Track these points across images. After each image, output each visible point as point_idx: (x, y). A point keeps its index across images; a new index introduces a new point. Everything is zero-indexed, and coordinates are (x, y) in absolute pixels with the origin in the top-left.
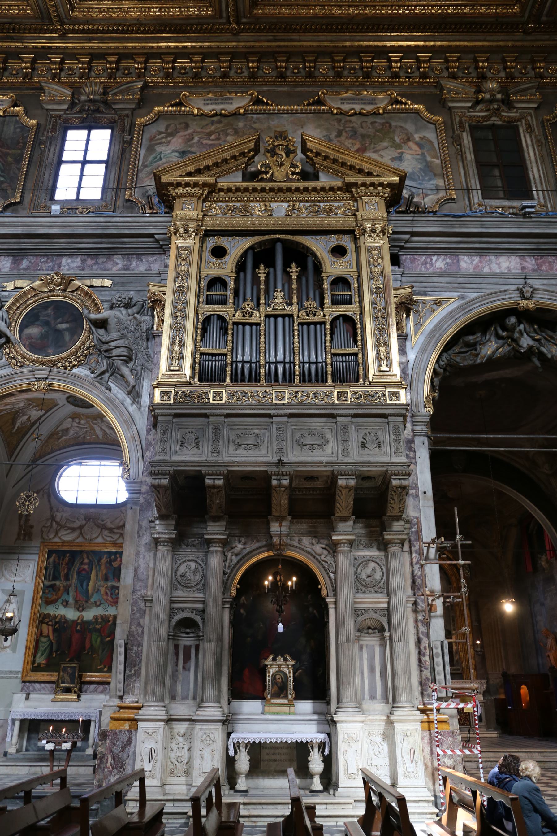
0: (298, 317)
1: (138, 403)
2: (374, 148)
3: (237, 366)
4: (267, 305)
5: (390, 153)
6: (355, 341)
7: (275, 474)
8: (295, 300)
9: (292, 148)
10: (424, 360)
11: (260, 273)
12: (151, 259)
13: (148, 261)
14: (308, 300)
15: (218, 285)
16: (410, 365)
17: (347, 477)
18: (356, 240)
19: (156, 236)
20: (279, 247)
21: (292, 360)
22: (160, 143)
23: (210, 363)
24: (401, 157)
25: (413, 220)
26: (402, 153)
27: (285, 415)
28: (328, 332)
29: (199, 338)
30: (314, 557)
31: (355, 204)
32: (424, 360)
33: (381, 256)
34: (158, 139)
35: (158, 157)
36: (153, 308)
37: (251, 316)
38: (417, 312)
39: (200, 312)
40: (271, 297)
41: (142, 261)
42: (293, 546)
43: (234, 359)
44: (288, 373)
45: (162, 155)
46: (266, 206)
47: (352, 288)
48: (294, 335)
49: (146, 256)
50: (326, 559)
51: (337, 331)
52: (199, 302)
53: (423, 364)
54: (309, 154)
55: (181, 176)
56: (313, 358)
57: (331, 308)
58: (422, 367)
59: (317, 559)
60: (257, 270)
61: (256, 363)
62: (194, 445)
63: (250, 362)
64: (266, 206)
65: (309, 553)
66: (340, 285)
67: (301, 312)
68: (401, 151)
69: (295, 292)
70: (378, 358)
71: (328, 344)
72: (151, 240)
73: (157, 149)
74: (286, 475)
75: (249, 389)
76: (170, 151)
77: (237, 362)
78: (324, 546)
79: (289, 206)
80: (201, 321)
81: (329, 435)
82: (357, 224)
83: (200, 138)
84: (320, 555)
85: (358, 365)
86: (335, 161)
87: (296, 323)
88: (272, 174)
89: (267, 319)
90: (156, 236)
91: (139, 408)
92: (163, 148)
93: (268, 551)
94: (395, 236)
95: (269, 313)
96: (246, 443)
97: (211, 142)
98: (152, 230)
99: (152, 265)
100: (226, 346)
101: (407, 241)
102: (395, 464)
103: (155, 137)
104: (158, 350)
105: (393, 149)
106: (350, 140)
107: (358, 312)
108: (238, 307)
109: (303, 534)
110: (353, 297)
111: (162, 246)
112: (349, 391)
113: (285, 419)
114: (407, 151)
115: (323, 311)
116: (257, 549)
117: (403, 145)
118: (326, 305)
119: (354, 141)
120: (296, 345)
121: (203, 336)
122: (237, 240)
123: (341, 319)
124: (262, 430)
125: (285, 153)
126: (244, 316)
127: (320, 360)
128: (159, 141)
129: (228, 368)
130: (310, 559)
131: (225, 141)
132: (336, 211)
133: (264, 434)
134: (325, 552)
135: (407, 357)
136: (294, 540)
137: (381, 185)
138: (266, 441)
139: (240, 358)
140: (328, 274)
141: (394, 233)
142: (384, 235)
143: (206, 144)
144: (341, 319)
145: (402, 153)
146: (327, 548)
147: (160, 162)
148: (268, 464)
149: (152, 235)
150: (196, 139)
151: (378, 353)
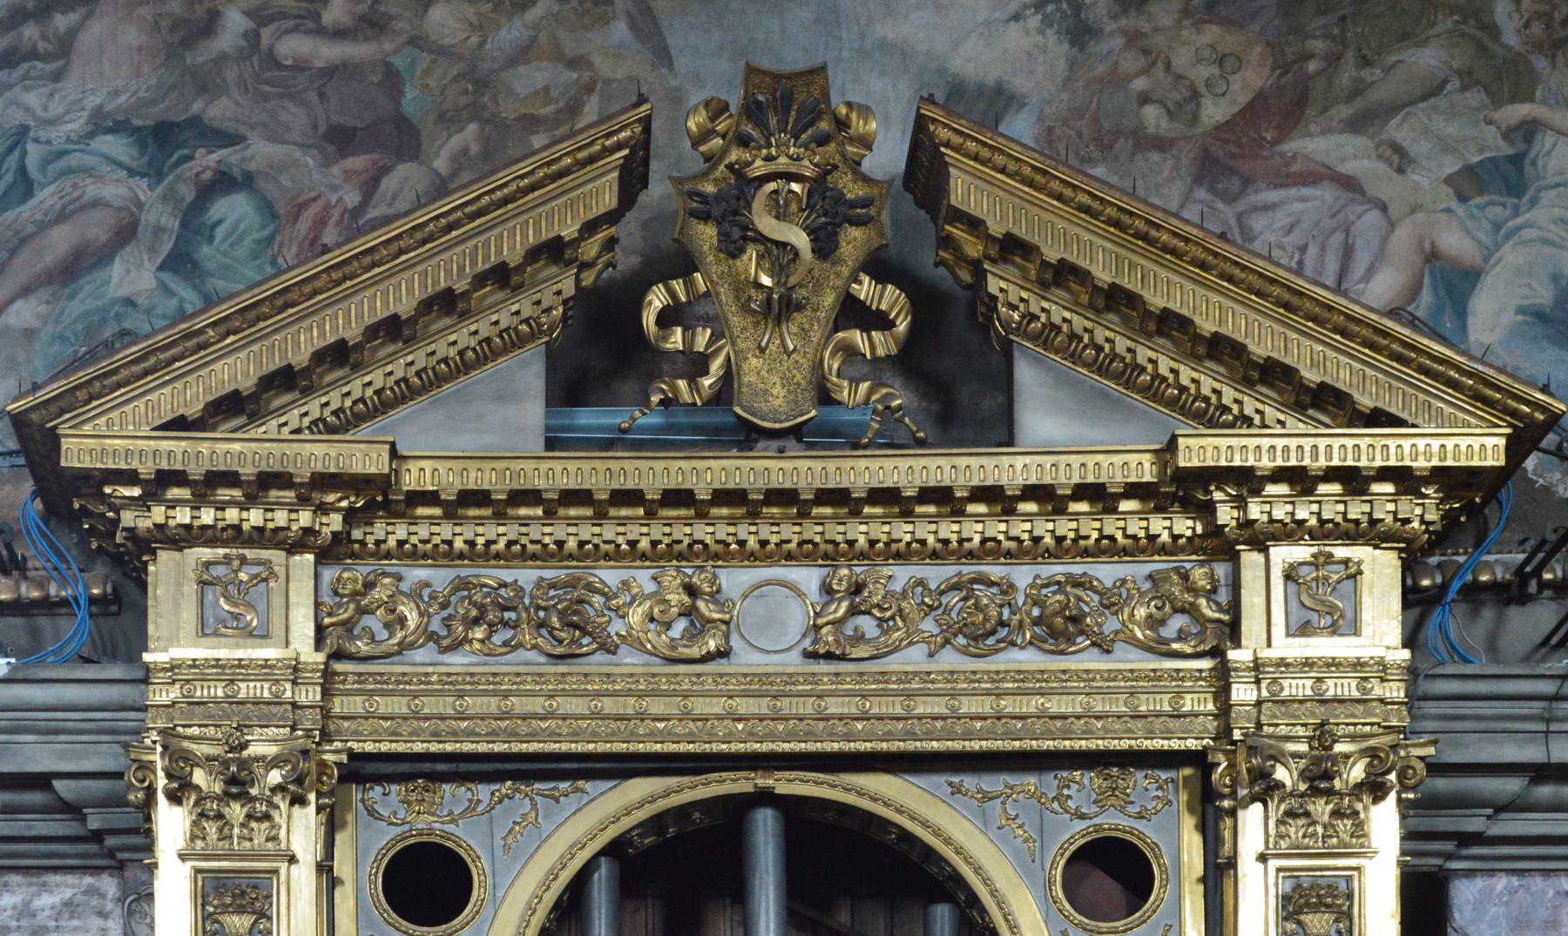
2: (1356, 92)
5: (1452, 129)
19: (57, 784)
24: (1517, 160)
26: (1529, 130)
31: (1221, 570)
45: (34, 154)
46: (691, 591)
68: (1518, 112)
76: (77, 125)
79: (827, 589)
83: (259, 16)
88: (728, 376)
90: (57, 784)
92: (33, 99)
97: (328, 52)
98: (38, 757)
105: (1476, 97)
106: (1212, 33)
117: (1540, 63)
119: (1230, 41)
132: (1111, 625)
141: (1436, 768)
143: (300, 66)
145: (1529, 130)
147: (26, 212)
150: (235, 22)
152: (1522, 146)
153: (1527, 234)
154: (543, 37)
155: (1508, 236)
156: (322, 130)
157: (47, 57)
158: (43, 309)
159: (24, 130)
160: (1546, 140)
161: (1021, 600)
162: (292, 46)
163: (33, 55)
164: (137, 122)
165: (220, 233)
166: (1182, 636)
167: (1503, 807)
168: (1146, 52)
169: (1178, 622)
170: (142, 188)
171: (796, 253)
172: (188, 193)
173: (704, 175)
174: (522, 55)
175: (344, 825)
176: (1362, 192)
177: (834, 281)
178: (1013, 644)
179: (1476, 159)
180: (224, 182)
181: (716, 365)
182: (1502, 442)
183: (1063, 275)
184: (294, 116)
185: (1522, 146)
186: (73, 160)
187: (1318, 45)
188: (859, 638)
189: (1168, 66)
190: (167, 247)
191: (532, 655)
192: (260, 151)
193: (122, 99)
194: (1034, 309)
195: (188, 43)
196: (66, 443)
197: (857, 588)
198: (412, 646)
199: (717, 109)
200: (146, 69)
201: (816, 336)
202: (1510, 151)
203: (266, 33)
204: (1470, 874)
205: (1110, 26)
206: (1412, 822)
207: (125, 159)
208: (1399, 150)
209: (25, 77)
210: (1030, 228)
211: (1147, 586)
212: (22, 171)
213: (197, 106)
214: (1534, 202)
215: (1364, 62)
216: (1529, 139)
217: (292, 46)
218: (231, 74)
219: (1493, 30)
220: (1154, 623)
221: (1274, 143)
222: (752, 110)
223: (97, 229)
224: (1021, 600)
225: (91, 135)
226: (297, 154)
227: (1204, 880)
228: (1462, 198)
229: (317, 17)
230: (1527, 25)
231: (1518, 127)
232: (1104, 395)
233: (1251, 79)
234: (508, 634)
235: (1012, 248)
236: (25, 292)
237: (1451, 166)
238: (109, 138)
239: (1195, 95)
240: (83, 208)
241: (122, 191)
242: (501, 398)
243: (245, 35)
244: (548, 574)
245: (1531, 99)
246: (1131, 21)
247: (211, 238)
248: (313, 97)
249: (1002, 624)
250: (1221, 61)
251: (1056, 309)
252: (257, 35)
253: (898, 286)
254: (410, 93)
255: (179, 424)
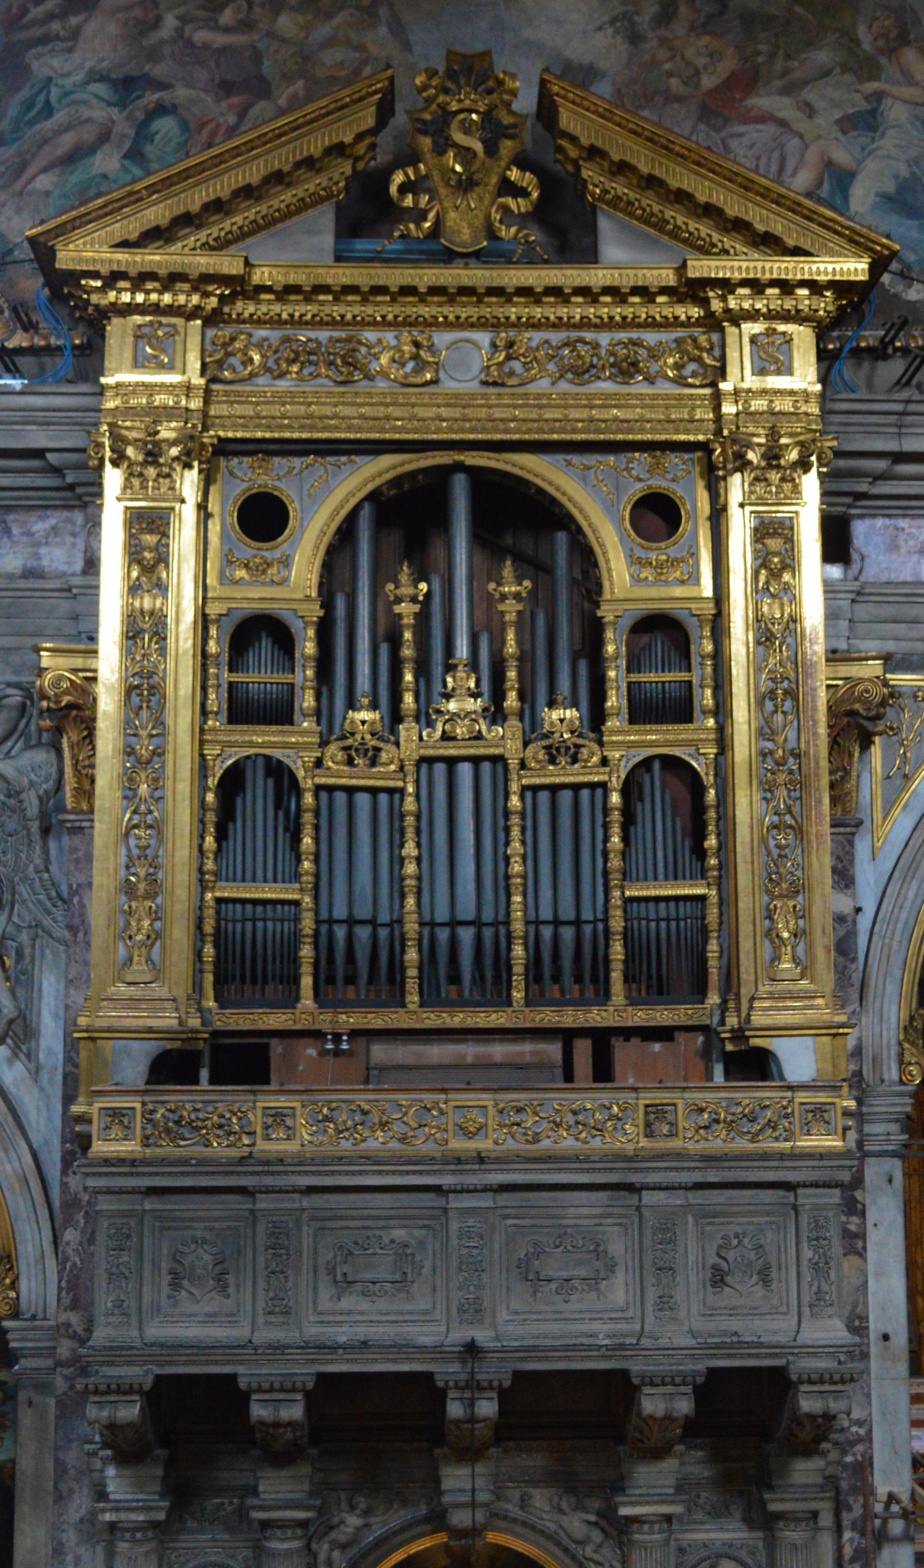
1: (28, 1056)
2: (784, 74)
3: (331, 935)
4: (424, 717)
6: (700, 854)
7: (457, 1387)
8: (511, 701)
9: (507, 120)
10: (908, 903)
12: (40, 526)
13: (30, 534)
14: (552, 704)
15: (266, 643)
16: (864, 922)
17: (669, 1389)
20: (460, 486)
21: (501, 918)
22: (44, 40)
23: (249, 925)
24: (873, 113)
25: (904, 413)
27: (486, 1189)
28: (616, 816)
29: (210, 841)
30: (566, 1550)
31: (715, 337)
32: (908, 903)
34: (35, 23)
35: (39, 105)
36: (58, 731)
37: (373, 763)
38: (895, 730)
39: (211, 751)
40: (438, 688)
41: (8, 531)
42: (505, 1518)
43: (324, 915)
44: (488, 961)
45: (54, 93)
46: (417, 345)
47: (695, 660)
48: (507, 830)
49: (21, 516)
50: (597, 1557)
51: (643, 810)
52: (204, 713)
53: (903, 916)
58: (900, 926)
59: (573, 1557)
60: (390, 586)
61: (390, 925)
62: (211, 1282)
63: (373, 922)
64: (417, 345)
65: (550, 1538)
66: (659, 644)
67: (531, 749)
68: (872, 86)
71: (615, 862)
72: (36, 463)
73: (35, 65)
74: (491, 1388)
76: (79, 77)
77: (331, 922)
78: (592, 1518)
79: (494, 345)
80: (212, 782)
81: (616, 1247)
82: (718, 432)
83: (184, 20)
84: (582, 1543)
85: (704, 933)
86: (652, 183)
87: (514, 787)
89: (424, 768)
91: (35, 1073)
92: (56, 63)
93: (434, 1532)
94: (842, 463)
95: (431, 752)
96: (369, 1276)
97: (220, 40)
98: (37, 439)
99: (43, 550)
101: (878, 478)
102: (813, 1350)
103: (24, 11)
104: (82, 879)
105: (848, 78)
106: (706, 39)
107: (712, 751)
108: (331, 731)
109: (533, 1482)
110: (696, 691)
111: (71, 487)
113: (485, 1201)
114: (895, 90)
115: (601, 744)
116: (402, 1530)
117: (883, 60)
118: (612, 723)
120: (516, 868)
121: (221, 836)
122: (320, 466)
123: (657, 766)
124: (416, 1232)
125: (484, 141)
126: (350, 762)
127: (587, 915)
128: (37, 32)
129: (306, 952)
130: (554, 1557)
131: (271, 35)
132: (654, 367)
133: (422, 1244)
134: (596, 1536)
135: (854, 896)
136: (508, 1500)
138: (426, 1270)
139: (340, 912)
140: (620, 608)
141: (838, 454)
143: (206, 46)
144: (657, 766)
145: (878, 97)
146: (603, 1523)
147: (48, 125)
148: (436, 1351)
149: (39, 454)
150: (170, 22)
152: (874, 105)
153: (880, 153)
154: (341, 34)
155: (869, 155)
156: (217, 81)
157: (65, 40)
158: (55, 179)
159: (50, 79)
160: (887, 102)
161: (603, 353)
162: (201, 36)
163: (58, 38)
164: (113, 76)
165: (158, 138)
166: (694, 375)
167: (878, 478)
168: (671, 49)
169: (692, 367)
170: (115, 112)
171: (475, 154)
172: (140, 116)
173: (424, 109)
174: (329, 43)
175: (215, 481)
176: (790, 128)
177: (497, 170)
178: (599, 378)
179: (851, 111)
180: (161, 110)
181: (431, 215)
182: (866, 266)
183: (622, 168)
184: (202, 75)
185: (874, 105)
186: (76, 96)
187: (763, 48)
188: (512, 373)
189: (683, 56)
190: (127, 145)
191: (324, 381)
192: (181, 93)
193: (105, 64)
194: (607, 187)
195: (143, 33)
196: (60, 255)
197: (510, 344)
198: (257, 375)
199: (432, 73)
200: (120, 47)
201: (487, 201)
202: (869, 107)
203: (187, 29)
204: (862, 517)
205: (650, 35)
206: (827, 485)
207: (105, 96)
208: (809, 105)
209: (52, 50)
210: (604, 143)
211: (674, 345)
212: (47, 102)
213: (147, 68)
214: (883, 135)
215: (788, 57)
216: (879, 101)
217: (201, 36)
218: (167, 50)
219: (858, 43)
220: (678, 366)
221: (741, 100)
222: (451, 74)
223: (88, 134)
224: (603, 353)
225: (86, 83)
226: (202, 95)
227: (710, 518)
228: (844, 133)
229: (216, 21)
230: (875, 39)
231: (871, 95)
232: (647, 236)
233: (727, 66)
234: (312, 368)
235: (594, 153)
236: (45, 170)
237: (838, 115)
238: (98, 85)
239: (697, 73)
240: (81, 123)
241: (104, 114)
242: (309, 232)
243: (176, 29)
244: (336, 334)
245: (879, 79)
246: (662, 32)
247: (152, 141)
248: (212, 64)
249: (593, 366)
250: (711, 55)
251: (619, 188)
252: (182, 29)
253: (532, 172)
254: (266, 63)
255: (124, 244)
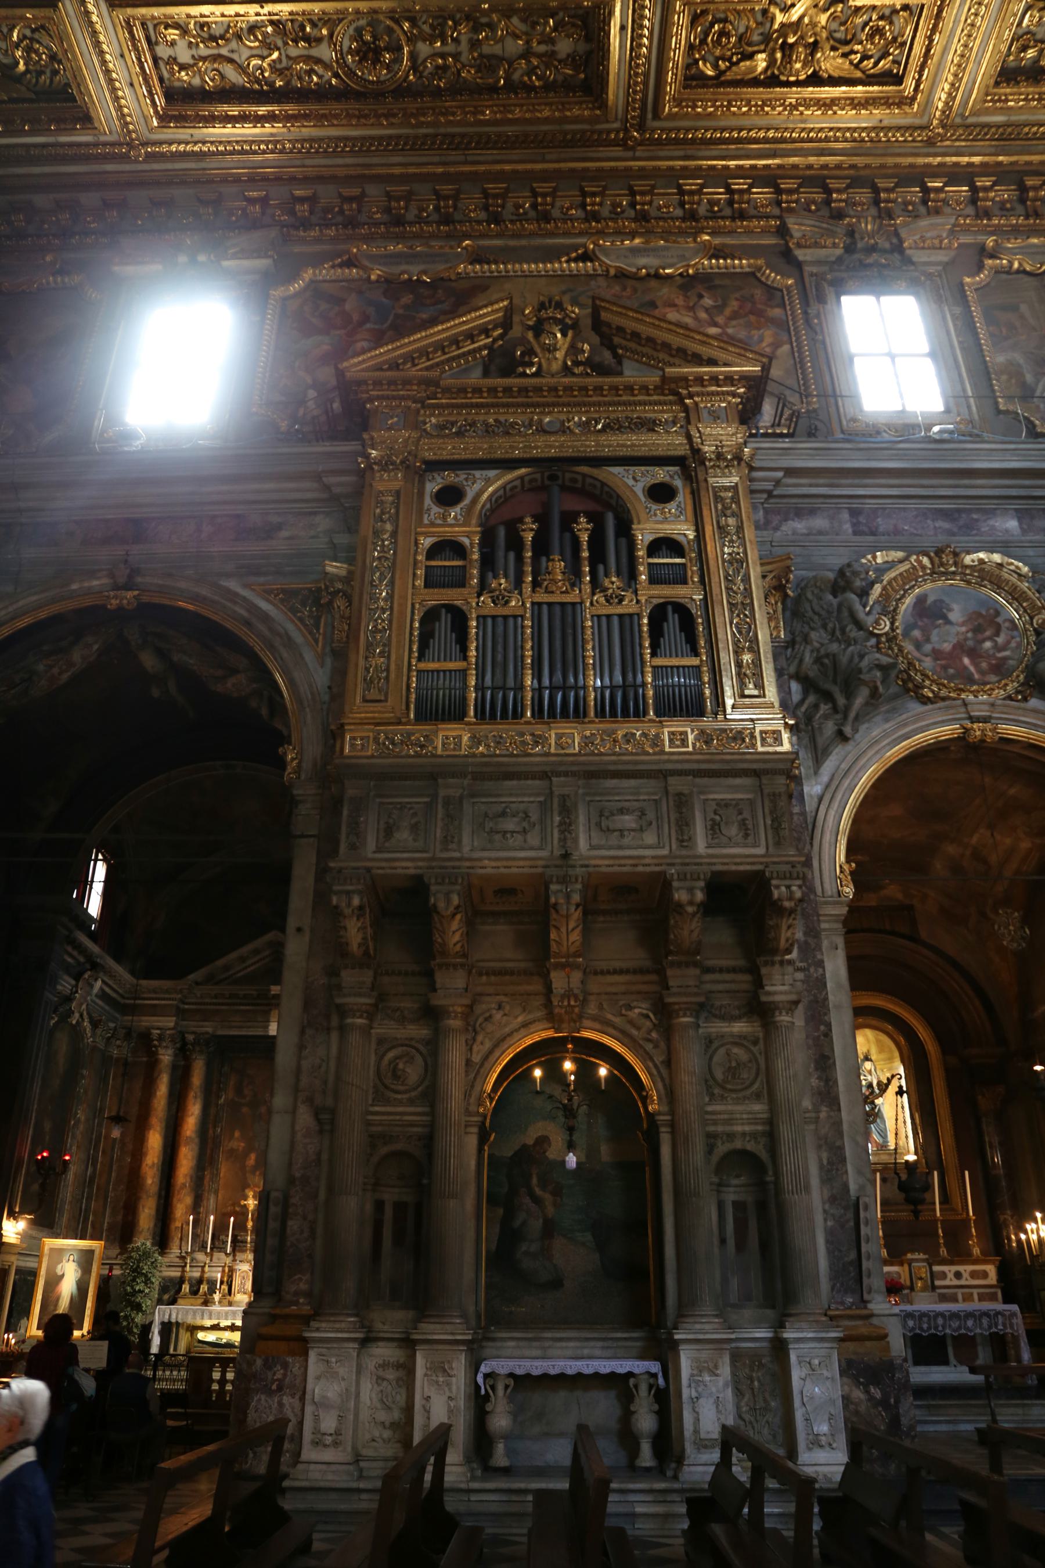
0: (592, 604)
11: (524, 530)
18: (688, 476)
33: (736, 499)
54: (604, 329)
55: (381, 369)
56: (618, 678)
57: (649, 590)
69: (586, 563)
70: (738, 674)
75: (507, 730)
100: (465, 658)
112: (689, 730)
137: (729, 379)
142: (739, 464)
151: (739, 665)
